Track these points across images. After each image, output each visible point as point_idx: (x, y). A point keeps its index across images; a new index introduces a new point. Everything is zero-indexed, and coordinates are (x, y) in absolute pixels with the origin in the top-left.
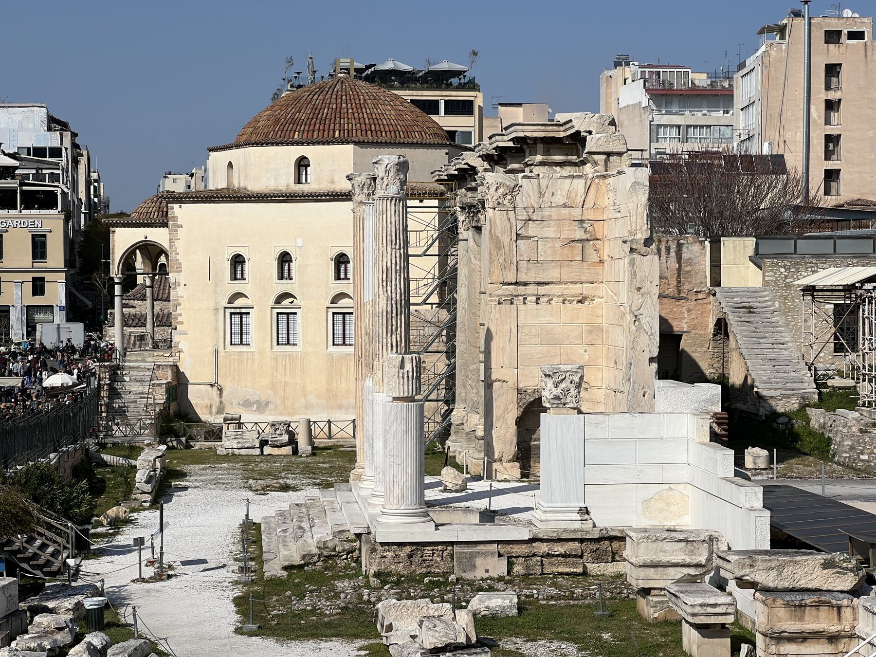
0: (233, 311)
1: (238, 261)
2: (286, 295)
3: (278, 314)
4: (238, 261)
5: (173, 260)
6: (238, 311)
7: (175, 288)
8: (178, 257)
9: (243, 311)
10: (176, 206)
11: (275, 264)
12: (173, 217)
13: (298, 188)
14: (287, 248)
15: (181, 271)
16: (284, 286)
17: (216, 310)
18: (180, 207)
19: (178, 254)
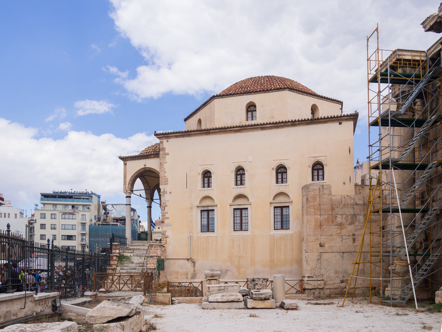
0: (203, 209)
1: (207, 175)
2: (240, 196)
3: (234, 209)
4: (207, 175)
5: (163, 177)
6: (206, 209)
7: (164, 195)
8: (166, 174)
9: (210, 208)
10: (165, 141)
11: (233, 175)
12: (162, 148)
13: (250, 122)
14: (241, 163)
15: (167, 184)
16: (240, 190)
17: (191, 208)
18: (168, 141)
19: (166, 172)
